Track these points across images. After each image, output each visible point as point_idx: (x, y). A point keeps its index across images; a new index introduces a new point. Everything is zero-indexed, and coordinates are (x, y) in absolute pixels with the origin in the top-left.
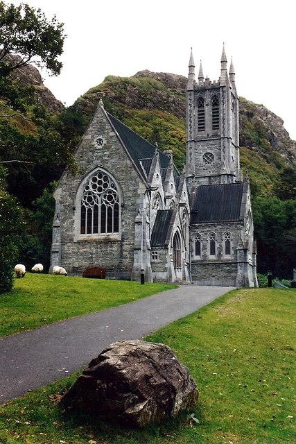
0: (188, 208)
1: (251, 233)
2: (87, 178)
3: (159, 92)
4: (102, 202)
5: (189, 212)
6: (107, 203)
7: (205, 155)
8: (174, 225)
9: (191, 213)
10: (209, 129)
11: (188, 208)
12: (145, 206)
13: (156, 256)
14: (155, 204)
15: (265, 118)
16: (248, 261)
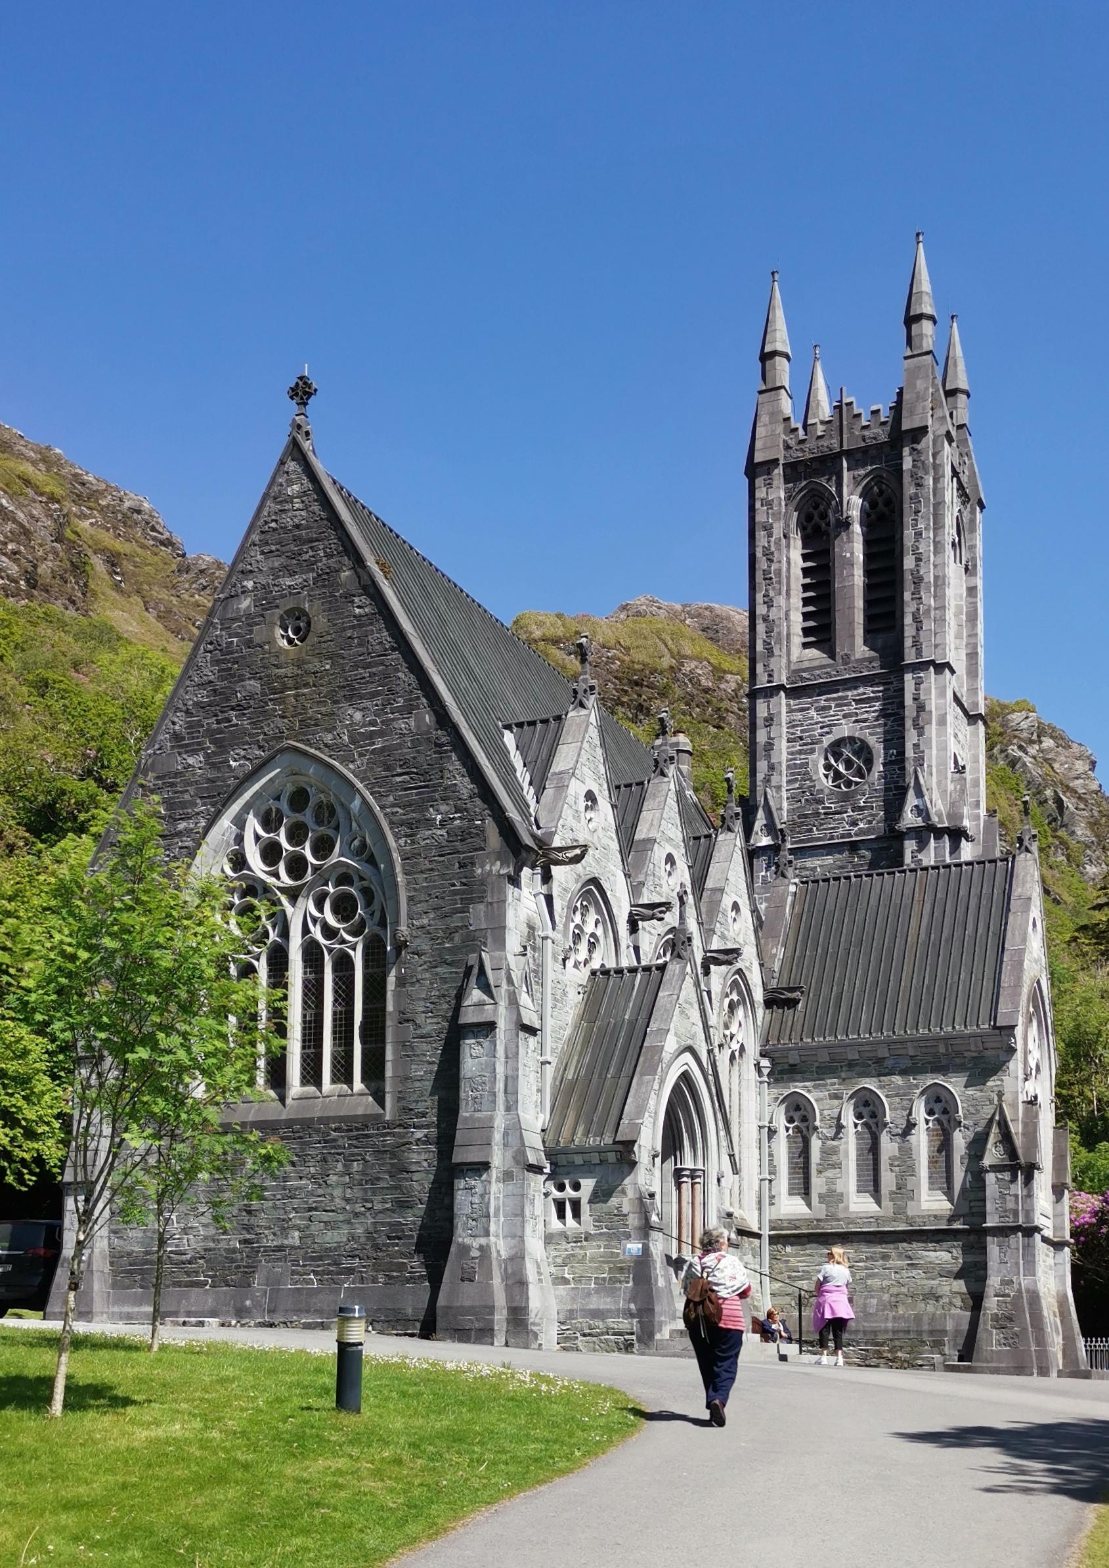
0: (755, 978)
1: (1043, 1088)
2: (235, 808)
3: (688, 666)
4: (306, 930)
5: (759, 995)
6: (329, 932)
7: (835, 749)
8: (671, 1044)
9: (769, 1004)
10: (857, 647)
11: (755, 978)
12: (513, 942)
13: (576, 1204)
14: (577, 938)
15: (1033, 750)
16: (1039, 1221)
